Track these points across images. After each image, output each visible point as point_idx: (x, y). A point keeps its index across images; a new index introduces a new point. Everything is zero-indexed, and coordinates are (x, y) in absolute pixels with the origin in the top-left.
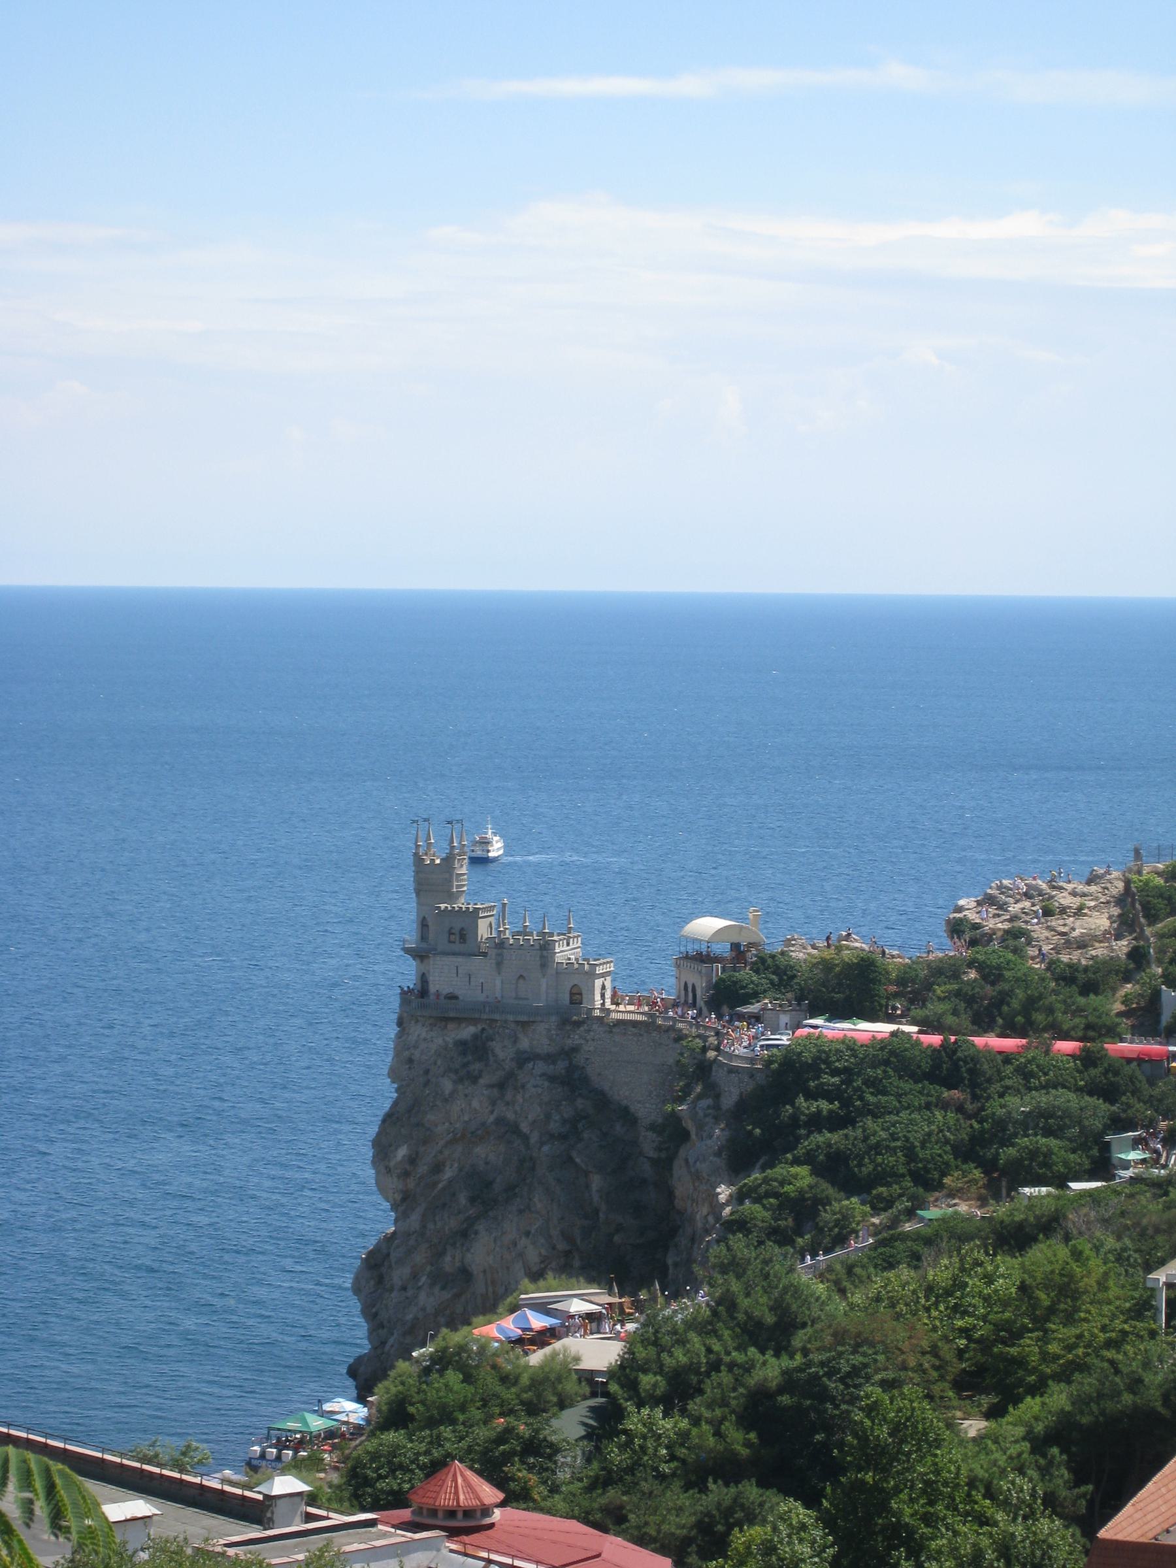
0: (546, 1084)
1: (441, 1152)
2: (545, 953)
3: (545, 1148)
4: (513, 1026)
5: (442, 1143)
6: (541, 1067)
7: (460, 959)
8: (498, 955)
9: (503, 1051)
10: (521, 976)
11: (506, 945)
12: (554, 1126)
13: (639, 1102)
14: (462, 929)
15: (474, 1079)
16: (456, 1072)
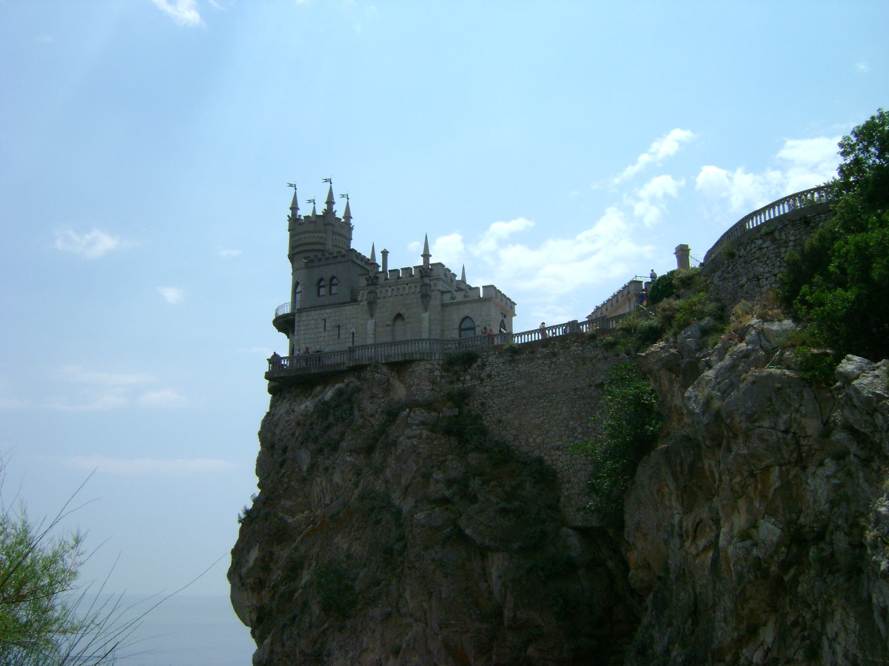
0: (425, 433)
1: (296, 549)
2: (427, 280)
3: (420, 516)
4: (385, 369)
5: (299, 538)
6: (419, 415)
7: (328, 311)
8: (370, 292)
9: (371, 407)
10: (399, 316)
11: (381, 280)
12: (437, 489)
13: (558, 448)
14: (333, 278)
15: (335, 447)
16: (316, 440)
